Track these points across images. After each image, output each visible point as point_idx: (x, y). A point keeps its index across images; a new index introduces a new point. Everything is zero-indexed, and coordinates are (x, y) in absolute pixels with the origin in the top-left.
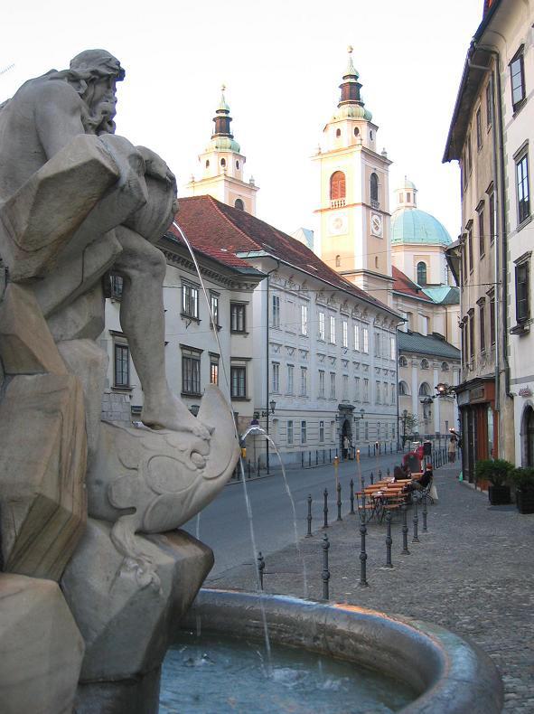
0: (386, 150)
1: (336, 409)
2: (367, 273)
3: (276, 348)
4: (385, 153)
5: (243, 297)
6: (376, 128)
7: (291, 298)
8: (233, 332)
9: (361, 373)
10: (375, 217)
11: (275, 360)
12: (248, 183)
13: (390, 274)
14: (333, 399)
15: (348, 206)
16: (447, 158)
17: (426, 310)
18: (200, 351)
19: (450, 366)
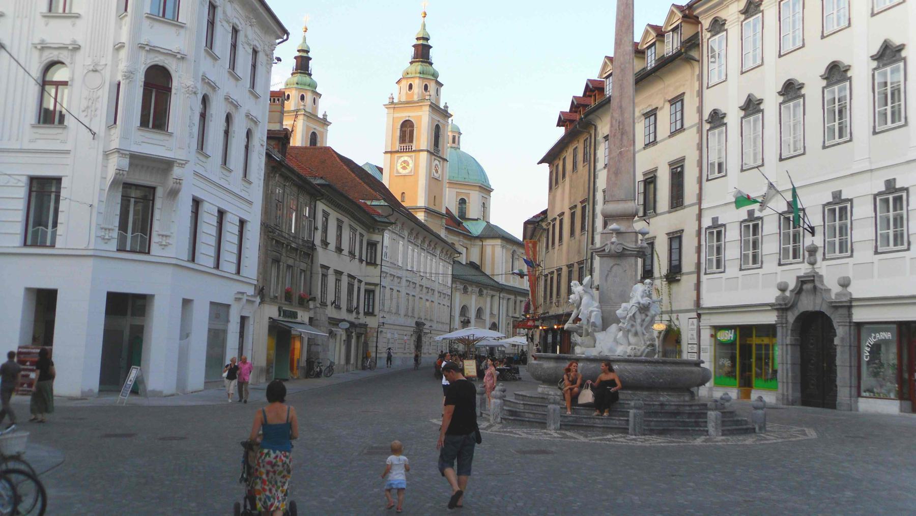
0: (448, 105)
1: (414, 325)
2: (428, 211)
3: (384, 275)
4: (447, 107)
5: (376, 237)
6: (441, 85)
7: (395, 236)
8: (368, 264)
10: (437, 162)
11: (384, 285)
12: (321, 117)
13: (444, 212)
14: (413, 317)
15: (414, 151)
17: (466, 241)
19: (485, 291)
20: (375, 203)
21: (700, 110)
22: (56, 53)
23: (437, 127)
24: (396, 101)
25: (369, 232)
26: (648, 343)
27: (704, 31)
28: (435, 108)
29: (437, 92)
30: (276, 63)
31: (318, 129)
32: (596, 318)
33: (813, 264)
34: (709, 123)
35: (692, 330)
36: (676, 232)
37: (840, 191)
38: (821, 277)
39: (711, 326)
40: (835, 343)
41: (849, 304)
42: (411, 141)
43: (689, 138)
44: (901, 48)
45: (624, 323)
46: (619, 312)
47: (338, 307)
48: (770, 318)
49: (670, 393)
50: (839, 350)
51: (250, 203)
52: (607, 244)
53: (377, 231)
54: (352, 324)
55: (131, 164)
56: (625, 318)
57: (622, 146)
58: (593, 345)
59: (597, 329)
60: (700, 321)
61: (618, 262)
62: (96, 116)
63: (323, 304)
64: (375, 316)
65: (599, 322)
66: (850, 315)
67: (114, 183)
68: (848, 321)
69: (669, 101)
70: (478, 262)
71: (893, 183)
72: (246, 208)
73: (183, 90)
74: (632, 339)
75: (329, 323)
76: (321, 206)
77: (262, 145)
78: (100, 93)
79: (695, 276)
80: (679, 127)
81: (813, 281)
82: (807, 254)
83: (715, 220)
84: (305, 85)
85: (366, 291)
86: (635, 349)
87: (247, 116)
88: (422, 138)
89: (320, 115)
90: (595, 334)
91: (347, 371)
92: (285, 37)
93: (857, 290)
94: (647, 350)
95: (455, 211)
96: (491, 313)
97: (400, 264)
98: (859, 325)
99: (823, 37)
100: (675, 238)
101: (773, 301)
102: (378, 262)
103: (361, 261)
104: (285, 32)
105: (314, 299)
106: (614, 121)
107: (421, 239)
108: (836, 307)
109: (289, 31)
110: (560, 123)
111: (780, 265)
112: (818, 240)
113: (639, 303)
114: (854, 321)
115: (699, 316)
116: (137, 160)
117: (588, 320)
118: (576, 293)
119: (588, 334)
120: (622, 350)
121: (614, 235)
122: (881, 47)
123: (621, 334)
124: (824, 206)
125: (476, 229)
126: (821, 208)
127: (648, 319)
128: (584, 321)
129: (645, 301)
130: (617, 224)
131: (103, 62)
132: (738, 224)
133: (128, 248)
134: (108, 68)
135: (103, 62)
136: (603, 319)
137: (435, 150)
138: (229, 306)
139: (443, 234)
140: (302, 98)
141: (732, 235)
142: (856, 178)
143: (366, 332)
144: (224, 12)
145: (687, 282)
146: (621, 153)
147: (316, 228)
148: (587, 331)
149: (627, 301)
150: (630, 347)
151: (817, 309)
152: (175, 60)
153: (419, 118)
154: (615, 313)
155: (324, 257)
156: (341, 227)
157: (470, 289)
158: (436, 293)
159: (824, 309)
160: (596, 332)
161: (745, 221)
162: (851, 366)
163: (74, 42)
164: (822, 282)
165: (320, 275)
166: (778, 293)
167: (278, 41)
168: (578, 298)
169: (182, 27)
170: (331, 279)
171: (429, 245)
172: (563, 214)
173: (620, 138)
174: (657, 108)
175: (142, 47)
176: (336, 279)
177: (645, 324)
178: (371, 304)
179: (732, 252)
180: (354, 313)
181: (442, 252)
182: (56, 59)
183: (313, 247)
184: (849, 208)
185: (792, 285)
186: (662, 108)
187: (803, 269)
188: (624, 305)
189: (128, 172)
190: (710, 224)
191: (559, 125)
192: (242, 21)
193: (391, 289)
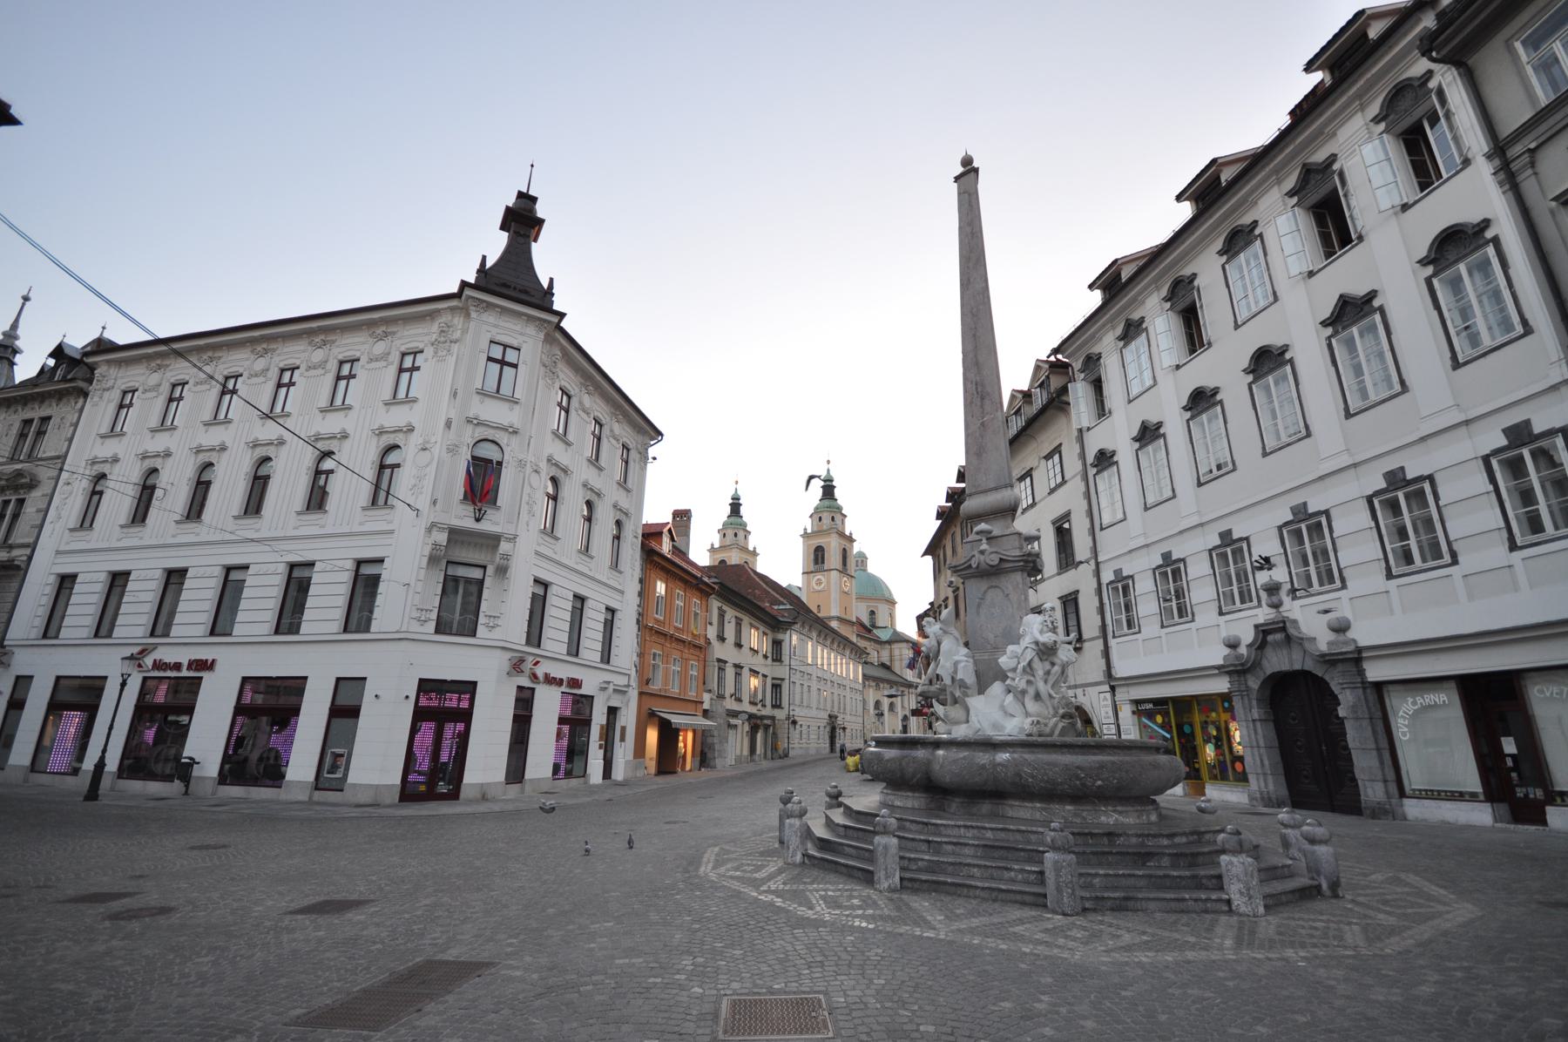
2: (840, 619)
5: (780, 636)
6: (845, 516)
9: (840, 691)
13: (854, 620)
16: (925, 554)
20: (781, 607)
21: (1083, 456)
22: (392, 436)
23: (844, 550)
24: (809, 531)
25: (773, 631)
26: (1061, 711)
27: (1076, 372)
28: (842, 535)
29: (843, 523)
31: (749, 558)
32: (967, 674)
33: (1276, 606)
34: (1096, 466)
35: (1106, 706)
36: (1070, 594)
37: (1305, 504)
38: (1295, 622)
39: (1131, 701)
40: (1342, 712)
41: (1356, 656)
42: (823, 562)
43: (1075, 487)
44: (1372, 295)
45: (1014, 679)
46: (1004, 661)
47: (739, 700)
48: (1221, 685)
49: (1119, 808)
50: (1348, 726)
51: (622, 592)
52: (974, 556)
54: (751, 716)
55: (449, 540)
56: (1014, 670)
57: (983, 414)
58: (964, 718)
59: (969, 692)
60: (1114, 695)
61: (994, 581)
62: (421, 493)
63: (721, 697)
65: (970, 679)
66: (1361, 672)
67: (433, 560)
68: (1359, 680)
69: (1045, 457)
70: (888, 664)
71: (1401, 475)
72: (619, 598)
73: (514, 464)
74: (1031, 706)
76: (715, 604)
78: (428, 469)
79: (1101, 640)
80: (1059, 479)
81: (1284, 629)
82: (1263, 595)
83: (1118, 572)
85: (773, 685)
86: (1038, 722)
87: (585, 485)
88: (833, 559)
89: (751, 548)
90: (966, 699)
91: (752, 761)
93: (1364, 634)
94: (1061, 725)
95: (866, 621)
96: (903, 707)
97: (810, 662)
98: (1379, 687)
99: (1237, 327)
100: (1070, 602)
101: (1220, 662)
102: (785, 658)
103: (765, 657)
104: (660, 433)
105: (710, 691)
106: (969, 386)
107: (823, 636)
108: (1330, 660)
110: (937, 519)
111: (1221, 613)
112: (1279, 574)
113: (1037, 643)
114: (1369, 680)
115: (1113, 689)
116: (456, 535)
117: (953, 678)
118: (931, 635)
119: (955, 701)
120: (1014, 725)
121: (984, 541)
122: (1336, 305)
123: (1010, 697)
124: (1280, 528)
125: (884, 635)
126: (1276, 531)
127: (1056, 669)
128: (947, 681)
129: (1047, 638)
130: (986, 523)
131: (433, 440)
132: (1151, 572)
133: (454, 631)
134: (438, 444)
135: (433, 440)
136: (978, 674)
137: (844, 568)
138: (592, 697)
139: (854, 639)
140: (736, 535)
141: (1144, 587)
142: (1328, 481)
143: (774, 724)
144: (581, 403)
145: (1093, 649)
147: (711, 624)
148: (953, 695)
149: (1016, 640)
150: (1029, 720)
151: (1297, 667)
152: (507, 434)
153: (830, 542)
154: (998, 664)
155: (719, 651)
157: (882, 686)
158: (848, 688)
159: (1309, 666)
160: (968, 696)
161: (1159, 567)
162: (1378, 749)
163: (410, 425)
164: (1298, 628)
165: (716, 669)
166: (1227, 651)
167: (652, 443)
168: (934, 643)
170: (730, 672)
171: (839, 646)
172: (947, 598)
173: (979, 404)
174: (1032, 469)
175: (469, 421)
177: (1052, 679)
179: (1147, 605)
180: (759, 706)
181: (851, 652)
182: (392, 442)
183: (708, 642)
184: (1324, 523)
185: (1247, 636)
186: (1037, 467)
187: (1263, 614)
188: (1011, 648)
189: (446, 547)
190: (1112, 578)
191: (937, 519)
193: (802, 685)
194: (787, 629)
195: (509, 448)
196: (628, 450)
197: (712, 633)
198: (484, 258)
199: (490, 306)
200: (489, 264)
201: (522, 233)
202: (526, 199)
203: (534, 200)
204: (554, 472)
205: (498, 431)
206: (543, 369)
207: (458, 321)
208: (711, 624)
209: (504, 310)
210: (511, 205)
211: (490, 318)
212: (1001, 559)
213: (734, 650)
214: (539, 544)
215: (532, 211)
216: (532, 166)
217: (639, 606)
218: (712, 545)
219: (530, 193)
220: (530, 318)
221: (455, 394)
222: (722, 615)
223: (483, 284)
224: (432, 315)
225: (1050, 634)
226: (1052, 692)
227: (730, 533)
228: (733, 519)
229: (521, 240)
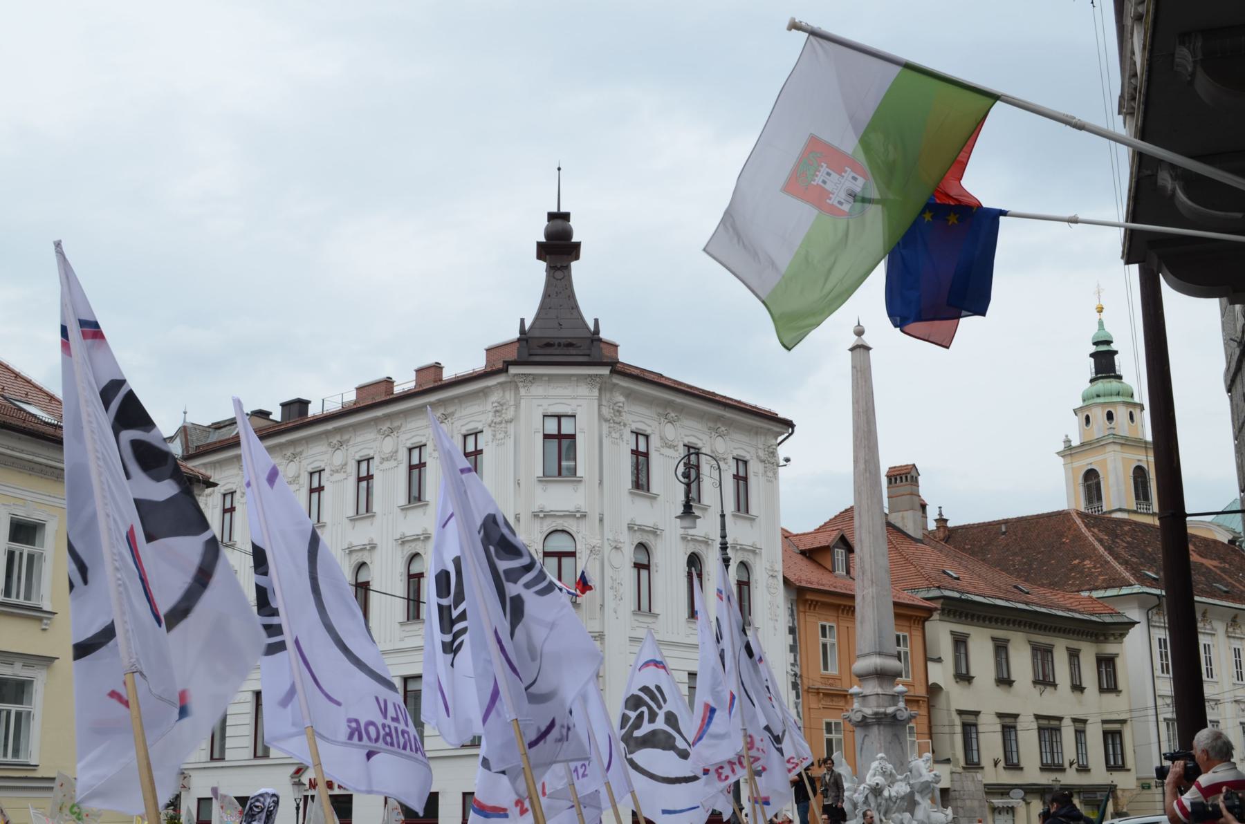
5: (1110, 648)
18: (1060, 719)
20: (1125, 591)
30: (785, 465)
53: (1112, 638)
63: (972, 764)
64: (1129, 770)
75: (987, 793)
77: (772, 576)
84: (1111, 395)
85: (1105, 733)
92: (790, 430)
104: (789, 424)
105: (948, 761)
109: (794, 422)
140: (1110, 416)
143: (1116, 798)
146: (863, 595)
156: (1006, 648)
165: (959, 729)
167: (780, 439)
169: (581, 481)
175: (535, 515)
176: (1004, 727)
178: (1119, 752)
192: (701, 436)
194: (1123, 635)
195: (580, 535)
196: (745, 463)
197: (940, 674)
198: (522, 321)
199: (535, 378)
200: (527, 325)
201: (559, 266)
202: (559, 218)
203: (566, 217)
204: (639, 538)
205: (566, 519)
206: (605, 426)
207: (509, 396)
208: (939, 660)
209: (551, 378)
210: (543, 239)
211: (538, 390)
212: (864, 717)
213: (1000, 692)
214: (633, 629)
215: (568, 233)
216: (559, 169)
217: (792, 665)
218: (1068, 441)
219: (563, 210)
220: (580, 378)
221: (519, 484)
222: (960, 642)
223: (525, 358)
224: (485, 392)
225: (880, 778)
226: (883, 818)
227: (1098, 415)
228: (1102, 385)
229: (559, 274)
